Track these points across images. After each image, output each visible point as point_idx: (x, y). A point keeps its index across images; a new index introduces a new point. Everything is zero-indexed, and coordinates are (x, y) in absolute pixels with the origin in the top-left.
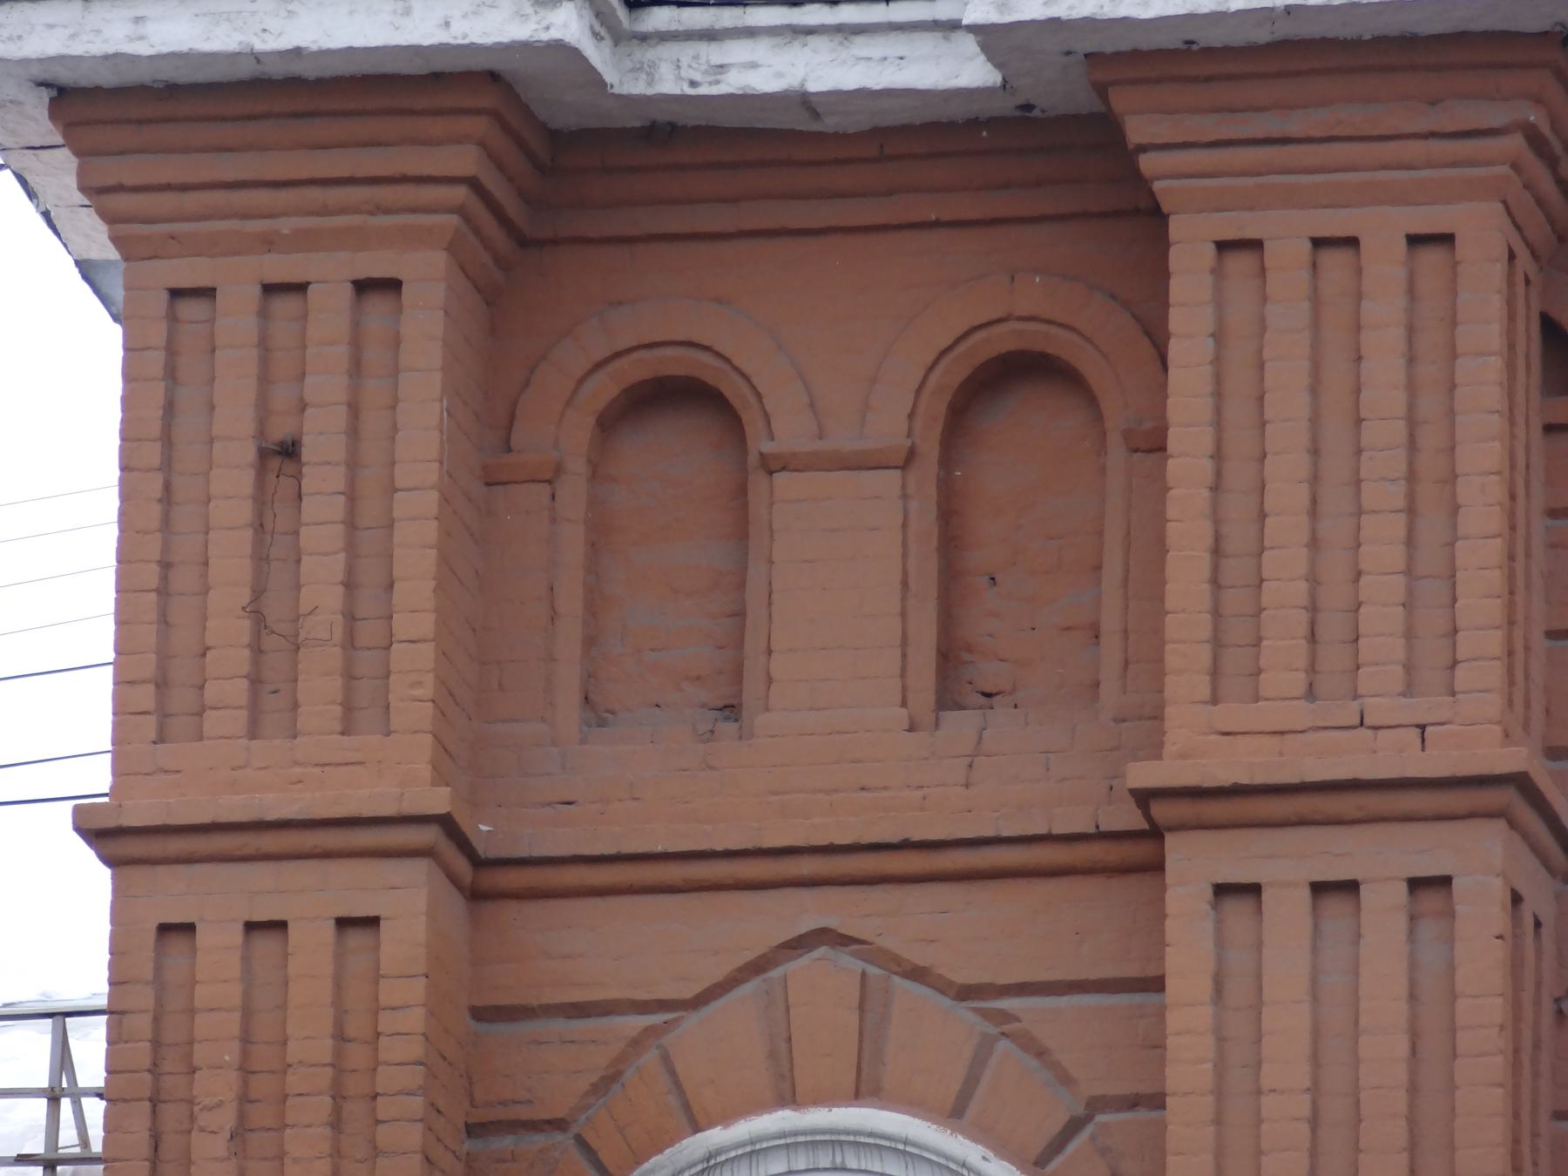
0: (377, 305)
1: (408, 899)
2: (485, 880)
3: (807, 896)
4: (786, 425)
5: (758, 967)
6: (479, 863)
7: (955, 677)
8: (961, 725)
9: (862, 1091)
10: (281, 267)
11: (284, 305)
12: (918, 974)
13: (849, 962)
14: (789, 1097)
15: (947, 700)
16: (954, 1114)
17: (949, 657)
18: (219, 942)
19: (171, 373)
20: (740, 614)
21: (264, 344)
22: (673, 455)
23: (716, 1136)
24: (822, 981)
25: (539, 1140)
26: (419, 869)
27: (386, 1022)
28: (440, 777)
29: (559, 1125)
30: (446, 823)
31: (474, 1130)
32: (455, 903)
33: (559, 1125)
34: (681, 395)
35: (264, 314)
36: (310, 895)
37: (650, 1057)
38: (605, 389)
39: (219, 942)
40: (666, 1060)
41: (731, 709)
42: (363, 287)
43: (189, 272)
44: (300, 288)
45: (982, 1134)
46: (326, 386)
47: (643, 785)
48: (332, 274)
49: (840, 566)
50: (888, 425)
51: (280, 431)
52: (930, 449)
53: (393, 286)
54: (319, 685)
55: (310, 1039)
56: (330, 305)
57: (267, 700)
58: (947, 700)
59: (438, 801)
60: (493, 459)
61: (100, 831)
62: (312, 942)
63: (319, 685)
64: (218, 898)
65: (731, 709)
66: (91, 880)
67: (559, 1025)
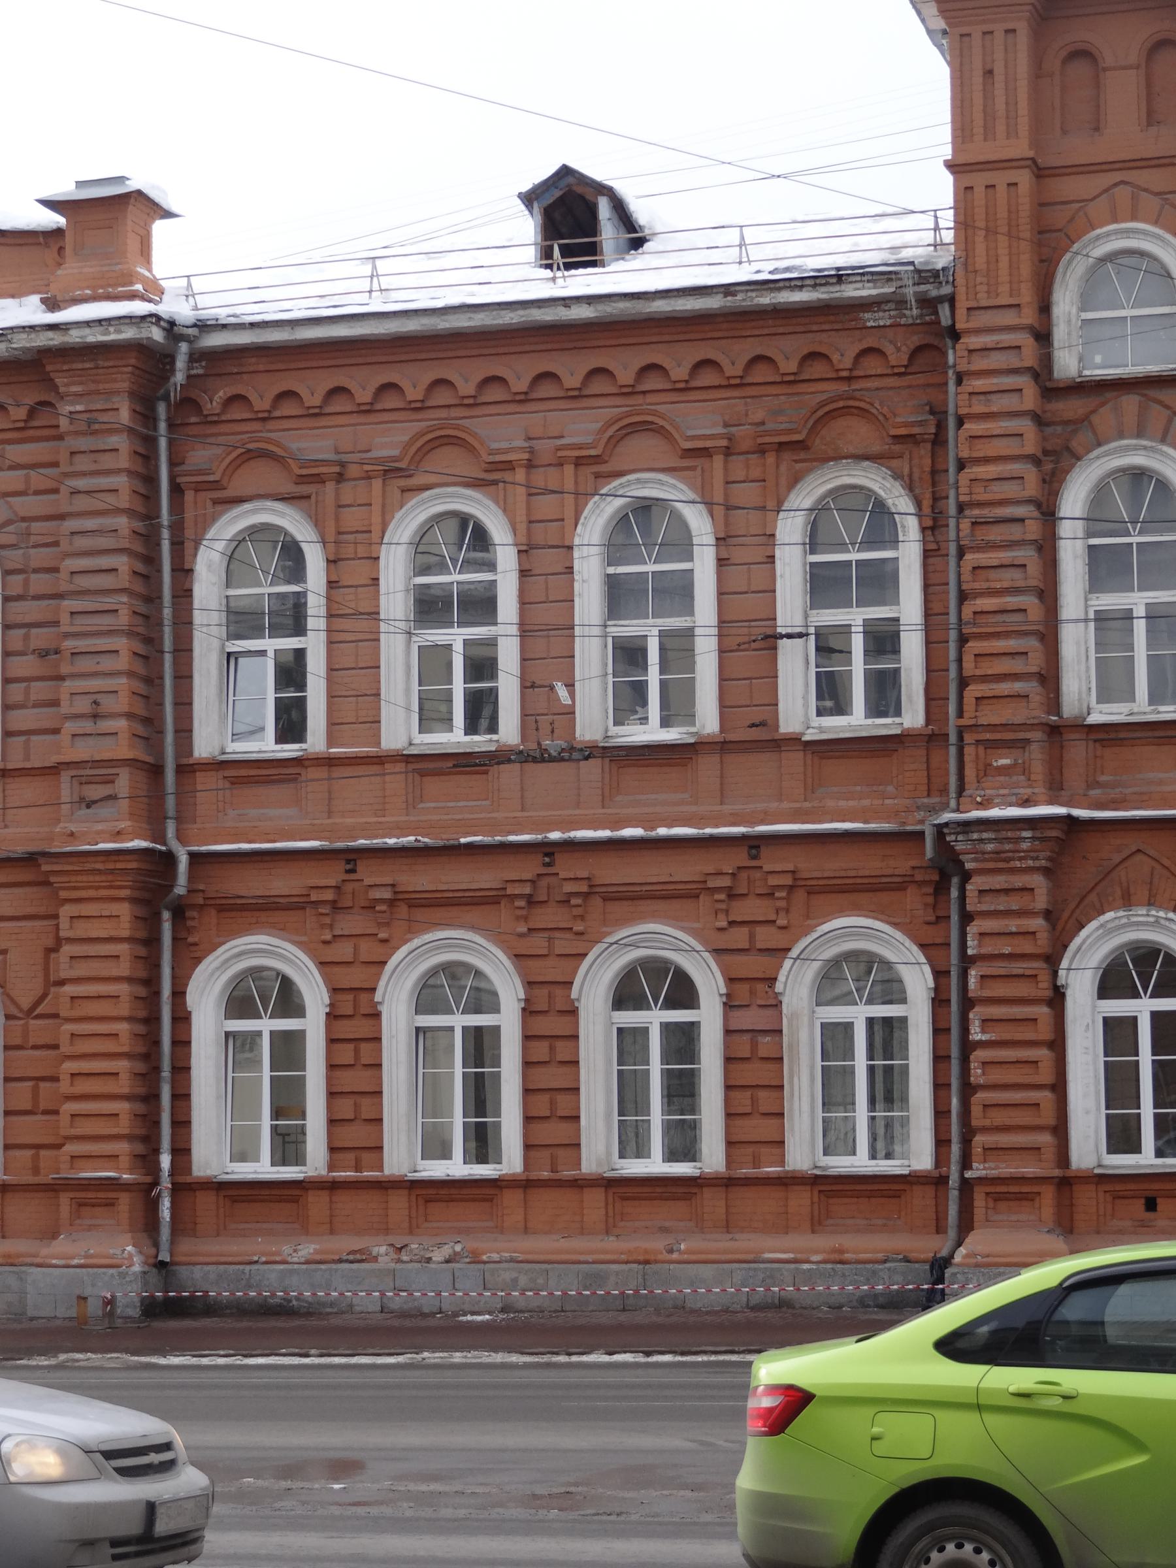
0: (1010, 36)
1: (1024, 178)
2: (1041, 173)
3: (1118, 173)
4: (1108, 59)
5: (1106, 191)
6: (1039, 169)
7: (1151, 118)
8: (1153, 130)
9: (1134, 218)
10: (987, 28)
11: (988, 37)
12: (1146, 190)
13: (1129, 189)
14: (1116, 221)
15: (1149, 124)
16: (1156, 223)
17: (1150, 113)
18: (1002, 189)
19: (961, 55)
20: (1098, 106)
21: (983, 46)
22: (1081, 69)
23: (1099, 231)
24: (1123, 193)
25: (1058, 234)
26: (1027, 170)
27: (1020, 208)
28: (1031, 149)
29: (1060, 230)
30: (1032, 159)
31: (1040, 233)
32: (1034, 179)
33: (1060, 230)
34: (1082, 54)
35: (983, 40)
36: (1001, 179)
37: (1081, 213)
38: (1064, 53)
39: (979, 191)
40: (1086, 214)
41: (1097, 129)
42: (1007, 31)
43: (965, 30)
44: (992, 32)
45: (1163, 227)
46: (999, 55)
47: (1077, 148)
48: (999, 28)
49: (1122, 94)
50: (1133, 58)
51: (988, 67)
52: (1144, 65)
53: (1014, 31)
54: (1001, 128)
55: (1002, 213)
56: (999, 36)
57: (989, 133)
58: (1149, 124)
59: (1031, 154)
60: (1038, 73)
61: (950, 166)
62: (1002, 189)
63: (1001, 128)
64: (979, 180)
65: (1097, 129)
66: (948, 179)
67: (1059, 207)
